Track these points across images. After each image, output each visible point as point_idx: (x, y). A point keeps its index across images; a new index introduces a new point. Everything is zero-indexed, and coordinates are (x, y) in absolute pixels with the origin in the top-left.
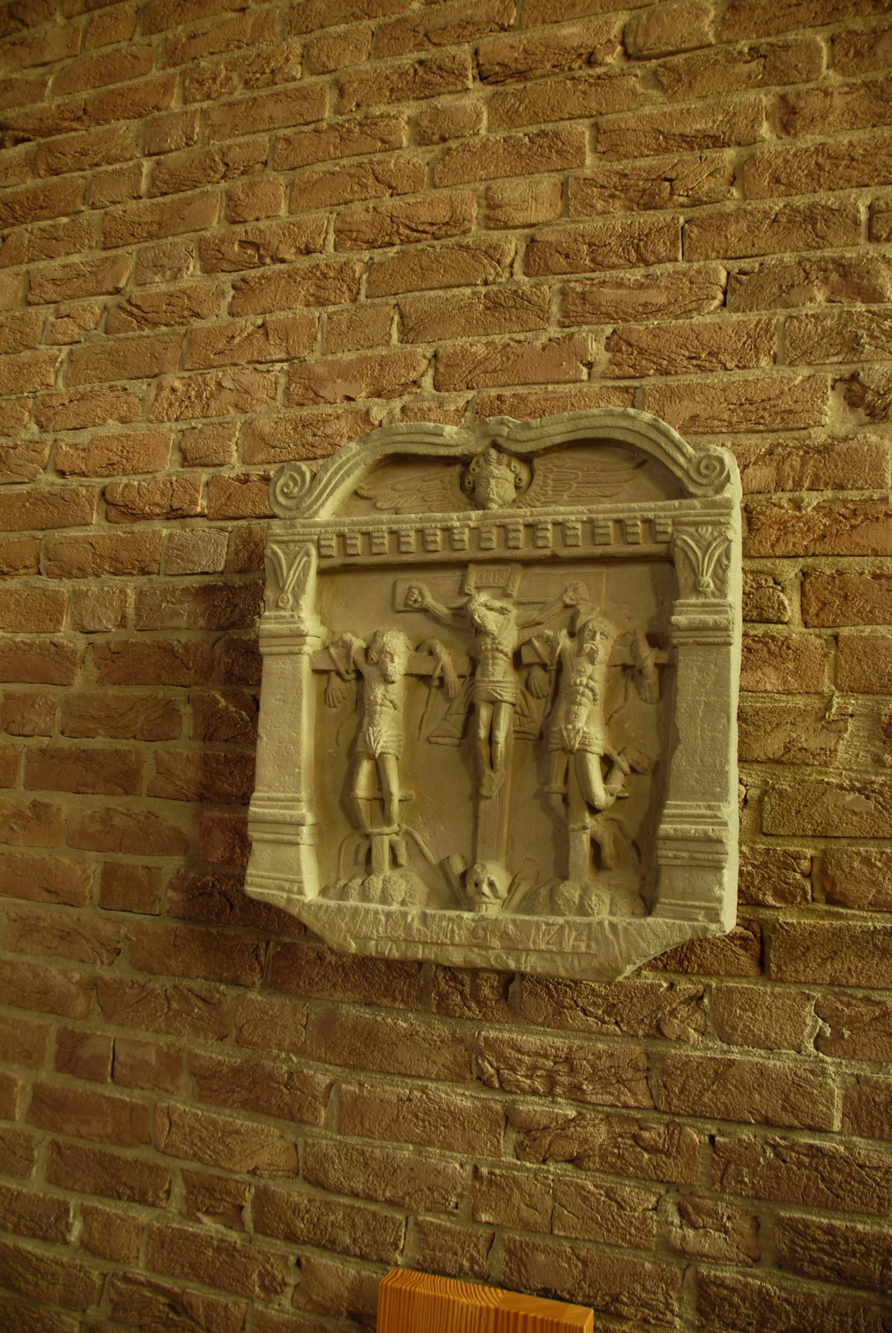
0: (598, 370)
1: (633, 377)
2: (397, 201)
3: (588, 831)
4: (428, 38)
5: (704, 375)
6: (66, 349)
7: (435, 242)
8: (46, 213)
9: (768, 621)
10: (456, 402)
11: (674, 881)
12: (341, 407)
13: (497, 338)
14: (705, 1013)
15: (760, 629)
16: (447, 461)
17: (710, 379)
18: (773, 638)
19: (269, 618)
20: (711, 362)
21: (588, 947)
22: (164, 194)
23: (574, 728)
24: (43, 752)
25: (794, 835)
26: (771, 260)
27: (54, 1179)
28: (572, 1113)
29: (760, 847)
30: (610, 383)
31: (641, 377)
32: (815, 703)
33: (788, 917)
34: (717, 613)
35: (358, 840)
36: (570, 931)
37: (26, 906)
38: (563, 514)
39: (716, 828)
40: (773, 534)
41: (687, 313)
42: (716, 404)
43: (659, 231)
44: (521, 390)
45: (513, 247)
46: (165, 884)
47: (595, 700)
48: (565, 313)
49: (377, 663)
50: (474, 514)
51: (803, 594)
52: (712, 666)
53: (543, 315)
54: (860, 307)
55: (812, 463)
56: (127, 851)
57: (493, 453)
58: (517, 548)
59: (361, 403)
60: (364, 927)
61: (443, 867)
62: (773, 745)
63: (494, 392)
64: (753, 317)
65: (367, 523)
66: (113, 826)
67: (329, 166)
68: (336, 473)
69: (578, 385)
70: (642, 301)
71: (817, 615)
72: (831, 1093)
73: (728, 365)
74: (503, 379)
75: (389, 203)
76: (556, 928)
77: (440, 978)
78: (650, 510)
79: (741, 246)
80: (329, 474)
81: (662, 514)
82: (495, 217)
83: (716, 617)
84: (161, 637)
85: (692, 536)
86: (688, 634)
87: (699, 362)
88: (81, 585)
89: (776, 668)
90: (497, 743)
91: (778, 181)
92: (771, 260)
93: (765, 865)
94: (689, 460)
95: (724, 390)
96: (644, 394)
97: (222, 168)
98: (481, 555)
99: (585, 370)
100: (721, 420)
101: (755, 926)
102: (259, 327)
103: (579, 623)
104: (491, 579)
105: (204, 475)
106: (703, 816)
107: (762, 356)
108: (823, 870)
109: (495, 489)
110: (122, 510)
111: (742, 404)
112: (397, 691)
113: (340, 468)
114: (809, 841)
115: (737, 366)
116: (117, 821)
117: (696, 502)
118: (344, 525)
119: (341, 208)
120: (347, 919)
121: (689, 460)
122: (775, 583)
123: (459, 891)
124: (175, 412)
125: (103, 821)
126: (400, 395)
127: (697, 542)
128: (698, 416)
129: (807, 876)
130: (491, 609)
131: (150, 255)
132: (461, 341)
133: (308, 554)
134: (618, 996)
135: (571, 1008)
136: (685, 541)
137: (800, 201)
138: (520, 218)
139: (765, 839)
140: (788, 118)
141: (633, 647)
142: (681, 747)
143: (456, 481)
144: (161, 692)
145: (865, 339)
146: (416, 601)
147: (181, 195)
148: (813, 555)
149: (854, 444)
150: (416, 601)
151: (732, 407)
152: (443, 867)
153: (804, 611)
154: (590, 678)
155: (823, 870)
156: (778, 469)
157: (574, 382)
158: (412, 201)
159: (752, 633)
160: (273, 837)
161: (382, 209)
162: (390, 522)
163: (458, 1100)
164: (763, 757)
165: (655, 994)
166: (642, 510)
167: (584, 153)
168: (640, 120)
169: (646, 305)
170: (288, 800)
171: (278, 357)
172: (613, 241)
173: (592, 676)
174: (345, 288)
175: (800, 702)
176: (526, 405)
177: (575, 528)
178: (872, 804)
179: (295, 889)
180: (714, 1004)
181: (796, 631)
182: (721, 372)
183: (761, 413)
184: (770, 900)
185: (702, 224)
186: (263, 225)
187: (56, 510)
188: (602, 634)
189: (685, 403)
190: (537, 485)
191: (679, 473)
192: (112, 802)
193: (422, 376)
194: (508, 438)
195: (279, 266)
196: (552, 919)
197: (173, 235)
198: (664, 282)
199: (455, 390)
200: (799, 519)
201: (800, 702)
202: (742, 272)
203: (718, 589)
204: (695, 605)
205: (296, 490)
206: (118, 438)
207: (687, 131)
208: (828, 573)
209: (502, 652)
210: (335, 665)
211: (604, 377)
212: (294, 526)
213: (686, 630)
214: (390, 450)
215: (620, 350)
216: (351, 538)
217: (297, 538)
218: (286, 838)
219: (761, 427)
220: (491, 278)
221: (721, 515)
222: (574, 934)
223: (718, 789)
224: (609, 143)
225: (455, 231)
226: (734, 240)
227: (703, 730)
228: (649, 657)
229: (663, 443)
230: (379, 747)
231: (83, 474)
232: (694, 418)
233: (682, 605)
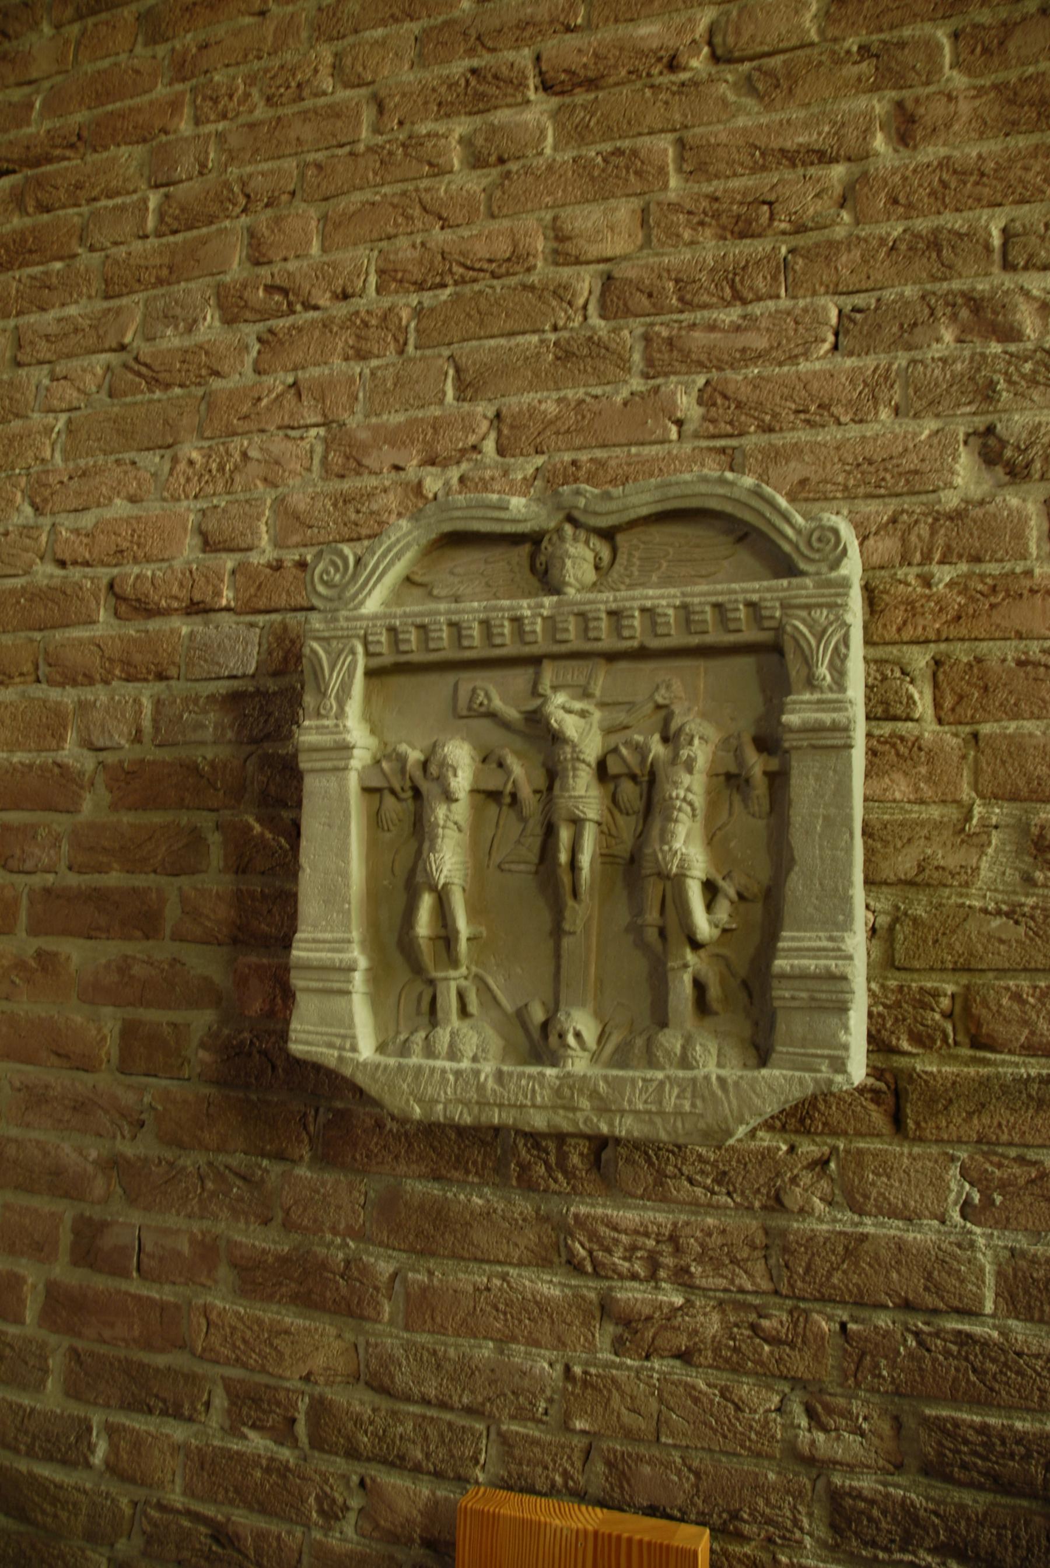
0: (689, 428)
1: (731, 436)
2: (449, 235)
4: (481, 42)
6: (63, 418)
7: (495, 282)
8: (36, 257)
9: (895, 718)
10: (523, 469)
11: (791, 1026)
12: (388, 478)
13: (570, 394)
15: (886, 728)
16: (515, 539)
18: (902, 739)
19: (310, 728)
21: (693, 1105)
22: (175, 232)
24: (47, 891)
25: (932, 969)
26: (889, 295)
27: (73, 1391)
28: (678, 1300)
29: (892, 984)
30: (704, 443)
32: (953, 813)
33: (926, 1065)
34: (835, 710)
35: (419, 986)
37: (32, 1073)
40: (900, 615)
41: (793, 359)
43: (758, 263)
44: (600, 454)
45: (586, 285)
46: (195, 1042)
47: (694, 816)
48: (649, 362)
50: (548, 601)
51: (936, 686)
53: (623, 364)
54: (995, 348)
55: (942, 531)
56: (149, 1005)
57: (568, 529)
59: (412, 473)
61: (521, 1015)
62: (905, 864)
63: (567, 457)
64: (870, 362)
65: (421, 614)
66: (132, 977)
67: (368, 195)
68: (384, 555)
70: (740, 346)
71: (953, 710)
72: (982, 1269)
73: (842, 419)
74: (578, 442)
75: (439, 237)
76: (655, 1084)
78: (754, 591)
79: (854, 278)
81: (768, 595)
82: (564, 250)
83: (835, 715)
85: (804, 621)
88: (88, 694)
89: (906, 774)
91: (895, 202)
92: (889, 295)
93: (898, 1004)
94: (799, 531)
95: (838, 448)
97: (242, 201)
98: (556, 648)
99: (674, 429)
101: (888, 1076)
102: (290, 386)
103: (674, 726)
105: (229, 562)
106: (824, 949)
108: (967, 1009)
110: (132, 605)
112: (461, 810)
113: (389, 550)
114: (949, 976)
116: (136, 970)
117: (808, 582)
119: (384, 244)
121: (799, 531)
122: (904, 673)
123: (541, 1043)
124: (194, 488)
126: (458, 463)
127: (810, 628)
129: (948, 1016)
130: (569, 711)
131: (160, 304)
132: (528, 398)
133: (353, 652)
136: (796, 628)
137: (922, 225)
138: (594, 251)
139: (897, 974)
140: (906, 128)
141: (738, 754)
142: (796, 869)
143: (526, 563)
144: (184, 819)
145: (1002, 385)
147: (195, 233)
148: (947, 640)
149: (991, 508)
152: (521, 1015)
153: (937, 705)
154: (688, 790)
155: (967, 1009)
156: (904, 540)
157: (662, 442)
158: (466, 233)
159: (877, 732)
160: (320, 985)
161: (432, 244)
162: (449, 612)
163: (545, 1288)
164: (892, 878)
166: (744, 591)
167: (667, 174)
168: (732, 132)
169: (743, 350)
170: (336, 941)
172: (704, 276)
173: (690, 788)
175: (935, 812)
178: (1022, 930)
180: (841, 1168)
181: (929, 730)
182: (834, 428)
183: (882, 474)
184: (905, 1045)
185: (808, 255)
186: (292, 266)
187: (56, 607)
189: (793, 464)
191: (787, 548)
192: (130, 948)
194: (585, 511)
195: (312, 314)
196: (649, 1074)
197: (187, 280)
198: (764, 323)
200: (929, 598)
201: (935, 812)
202: (856, 310)
204: (808, 702)
205: (338, 577)
206: (128, 521)
207: (788, 145)
208: (965, 660)
211: (696, 436)
212: (335, 620)
214: (447, 527)
215: (714, 404)
218: (336, 986)
219: (882, 491)
220: (561, 323)
221: (838, 595)
222: (676, 1091)
223: (841, 918)
224: (695, 159)
225: (517, 268)
226: (846, 273)
227: (821, 848)
228: (757, 764)
231: (87, 564)
232: (803, 482)
233: (794, 702)
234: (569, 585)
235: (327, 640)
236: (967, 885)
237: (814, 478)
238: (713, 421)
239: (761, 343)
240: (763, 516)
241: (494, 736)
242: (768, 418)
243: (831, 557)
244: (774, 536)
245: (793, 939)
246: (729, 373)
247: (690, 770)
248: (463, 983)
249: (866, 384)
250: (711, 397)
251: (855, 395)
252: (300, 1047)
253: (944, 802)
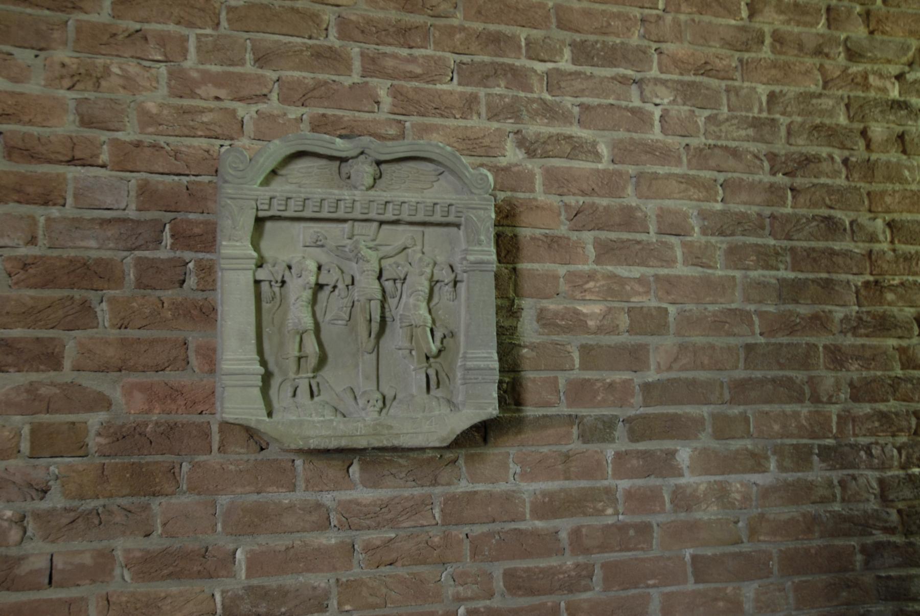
19: (226, 246)
26: (477, 58)
28: (393, 535)
41: (433, 82)
43: (417, 27)
48: (364, 69)
53: (349, 69)
54: (522, 94)
56: (57, 411)
64: (469, 89)
70: (409, 70)
73: (458, 116)
74: (326, 104)
84: (73, 253)
91: (480, 12)
102: (137, 31)
105: (104, 136)
117: (476, 198)
124: (67, 83)
125: (28, 391)
132: (297, 74)
137: (492, 27)
144: (77, 294)
145: (525, 113)
148: (503, 226)
149: (520, 168)
160: (241, 383)
163: (324, 541)
169: (411, 72)
171: (160, 58)
172: (392, 30)
174: (208, 19)
178: (534, 354)
182: (453, 119)
189: (435, 135)
192: (34, 376)
198: (421, 60)
220: (314, 35)
236: (512, 334)
239: (419, 71)
246: (402, 83)
253: (502, 298)
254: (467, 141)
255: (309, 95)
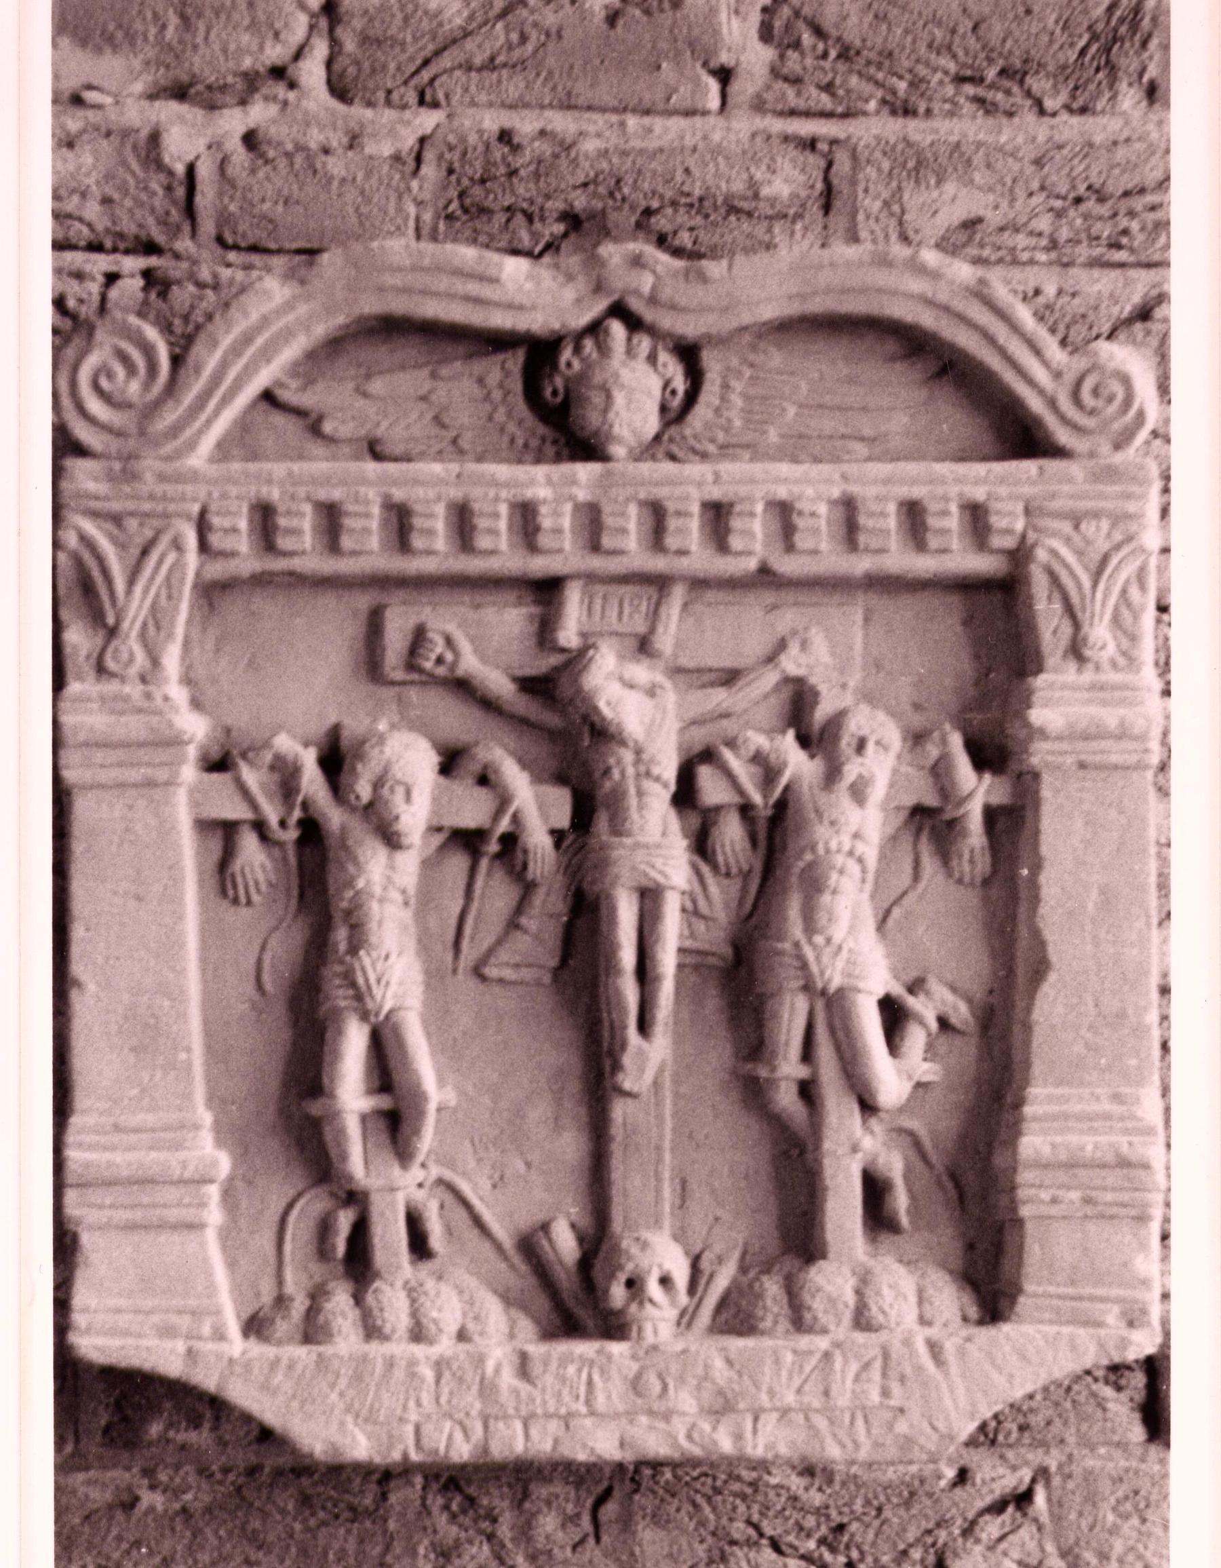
0: (744, 88)
3: (860, 1155)
5: (991, 121)
10: (392, 133)
11: (1050, 1247)
14: (1040, 1529)
17: (1008, 134)
20: (1008, 92)
21: (885, 1393)
23: (829, 940)
30: (778, 126)
31: (845, 115)
34: (1122, 702)
35: (314, 1204)
36: (846, 1362)
38: (786, 480)
39: (1135, 1139)
42: (1021, 193)
44: (562, 123)
47: (863, 881)
49: (370, 805)
50: (585, 471)
52: (1113, 813)
57: (617, 329)
58: (682, 552)
59: (137, 114)
60: (385, 1396)
61: (530, 1247)
63: (492, 121)
65: (327, 481)
68: (236, 350)
69: (698, 121)
73: (1049, 104)
76: (814, 1361)
77: (435, 1510)
78: (977, 482)
80: (218, 354)
83: (1122, 711)
86: (1065, 746)
87: (980, 91)
90: (657, 979)
94: (1057, 375)
95: (1038, 163)
96: (854, 156)
98: (597, 563)
99: (713, 86)
100: (1031, 233)
103: (822, 712)
104: (613, 614)
106: (1107, 1117)
107: (1123, 86)
109: (624, 414)
111: (1078, 200)
112: (408, 865)
113: (247, 339)
115: (1068, 108)
118: (269, 482)
120: (343, 1383)
123: (578, 1299)
126: (243, 102)
127: (1080, 553)
128: (980, 220)
130: (631, 686)
133: (177, 545)
134: (849, 1504)
135: (749, 1543)
136: (1054, 553)
141: (940, 772)
142: (1052, 977)
146: (440, 661)
150: (440, 661)
151: (1058, 204)
152: (530, 1247)
154: (856, 836)
157: (689, 113)
162: (383, 480)
165: (930, 1495)
166: (958, 480)
170: (166, 1128)
173: (855, 832)
176: (575, 162)
177: (813, 514)
179: (206, 1330)
180: (1055, 1504)
182: (1029, 117)
183: (1124, 222)
188: (878, 743)
189: (950, 188)
190: (708, 405)
191: (1035, 404)
193: (298, 55)
194: (653, 300)
196: (804, 1342)
199: (388, 103)
203: (1124, 654)
205: (134, 387)
209: (657, 779)
210: (255, 807)
211: (758, 106)
212: (131, 476)
213: (1059, 738)
214: (371, 306)
215: (797, 45)
216: (288, 513)
217: (147, 506)
218: (173, 1214)
219: (1122, 256)
221: (1128, 496)
222: (854, 1367)
223: (1133, 1062)
227: (1096, 941)
228: (977, 791)
229: (1001, 332)
230: (389, 994)
232: (971, 224)
233: (1051, 686)
234: (620, 441)
235: (117, 519)
237: (994, 218)
238: (795, 81)
240: (990, 339)
241: (456, 720)
242: (902, 86)
243: (1117, 426)
244: (1009, 377)
245: (1050, 1099)
247: (858, 793)
248: (419, 1195)
249: (1094, 37)
250: (788, 27)
251: (1072, 55)
252: (100, 1341)
254: (1090, 205)
255: (446, 61)
